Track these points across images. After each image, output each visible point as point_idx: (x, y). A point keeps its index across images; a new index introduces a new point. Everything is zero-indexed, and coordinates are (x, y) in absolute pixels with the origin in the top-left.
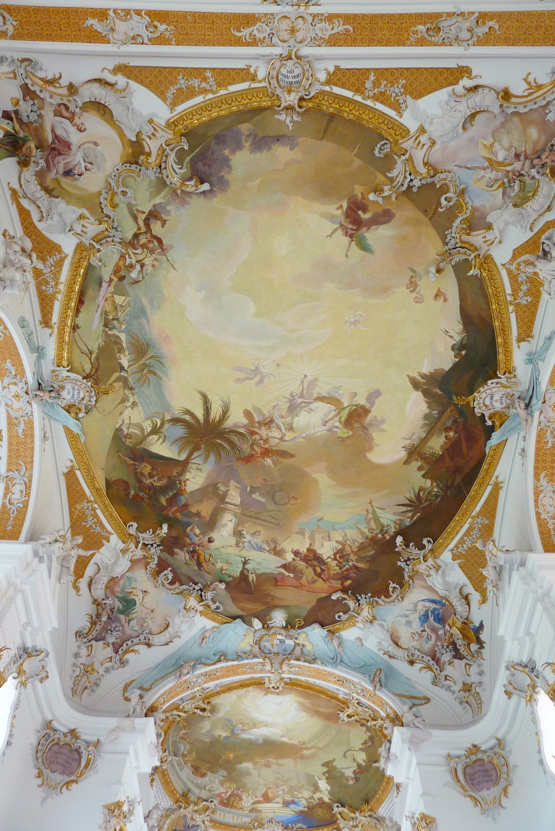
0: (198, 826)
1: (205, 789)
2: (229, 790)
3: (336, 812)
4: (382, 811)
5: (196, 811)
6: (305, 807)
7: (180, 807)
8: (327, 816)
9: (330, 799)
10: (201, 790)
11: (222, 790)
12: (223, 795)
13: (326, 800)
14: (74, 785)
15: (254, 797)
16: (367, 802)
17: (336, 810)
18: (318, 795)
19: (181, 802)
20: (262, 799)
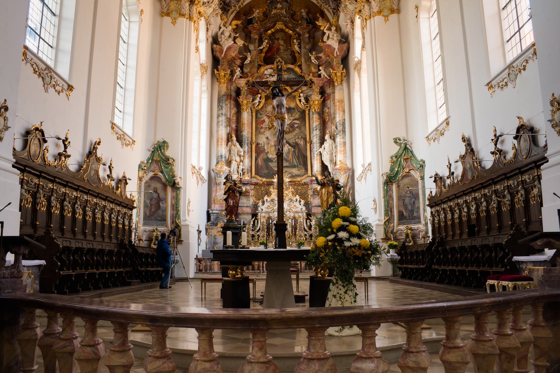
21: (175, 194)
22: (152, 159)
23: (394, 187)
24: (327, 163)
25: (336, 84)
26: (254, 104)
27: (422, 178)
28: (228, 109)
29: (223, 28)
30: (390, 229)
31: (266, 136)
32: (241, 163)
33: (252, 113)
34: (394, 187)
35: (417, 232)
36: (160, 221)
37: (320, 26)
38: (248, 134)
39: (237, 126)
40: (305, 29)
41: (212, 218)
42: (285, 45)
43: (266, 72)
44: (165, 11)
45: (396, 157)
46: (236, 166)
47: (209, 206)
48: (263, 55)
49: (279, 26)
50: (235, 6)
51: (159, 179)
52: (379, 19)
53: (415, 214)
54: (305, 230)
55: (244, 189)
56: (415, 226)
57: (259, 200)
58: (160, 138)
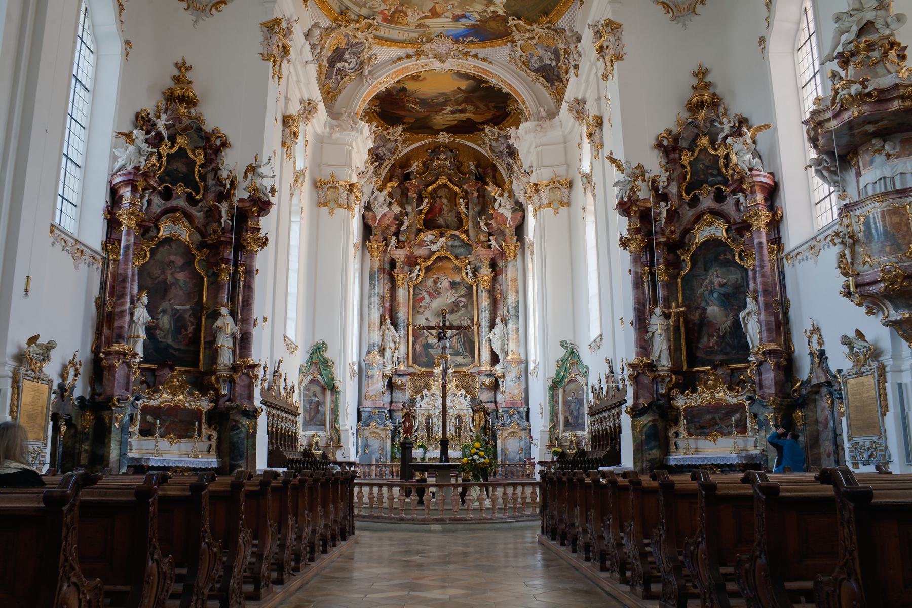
0: (362, 43)
1: (365, 7)
2: (392, 6)
3: (511, 25)
4: (562, 23)
5: (358, 29)
6: (477, 21)
7: (340, 26)
8: (501, 28)
9: (504, 12)
10: (361, 8)
11: (384, 7)
12: (386, 12)
13: (501, 13)
14: (223, 6)
15: (420, 13)
16: (546, 14)
17: (511, 22)
18: (492, 8)
19: (340, 21)
20: (429, 14)
21: (334, 397)
22: (310, 362)
23: (560, 392)
24: (497, 351)
25: (508, 259)
26: (411, 278)
27: (587, 384)
28: (382, 287)
29: (377, 193)
30: (556, 436)
31: (426, 316)
32: (397, 351)
33: (409, 288)
34: (560, 392)
35: (581, 439)
36: (320, 425)
37: (491, 191)
38: (404, 315)
39: (391, 305)
40: (474, 186)
41: (363, 416)
42: (449, 205)
43: (426, 239)
44: (322, 201)
45: (562, 361)
46: (390, 354)
47: (360, 403)
48: (423, 216)
49: (442, 181)
50: (389, 159)
51: (318, 382)
52: (548, 211)
53: (580, 421)
54: (471, 431)
55: (399, 382)
56: (579, 433)
57: (417, 393)
58: (318, 339)
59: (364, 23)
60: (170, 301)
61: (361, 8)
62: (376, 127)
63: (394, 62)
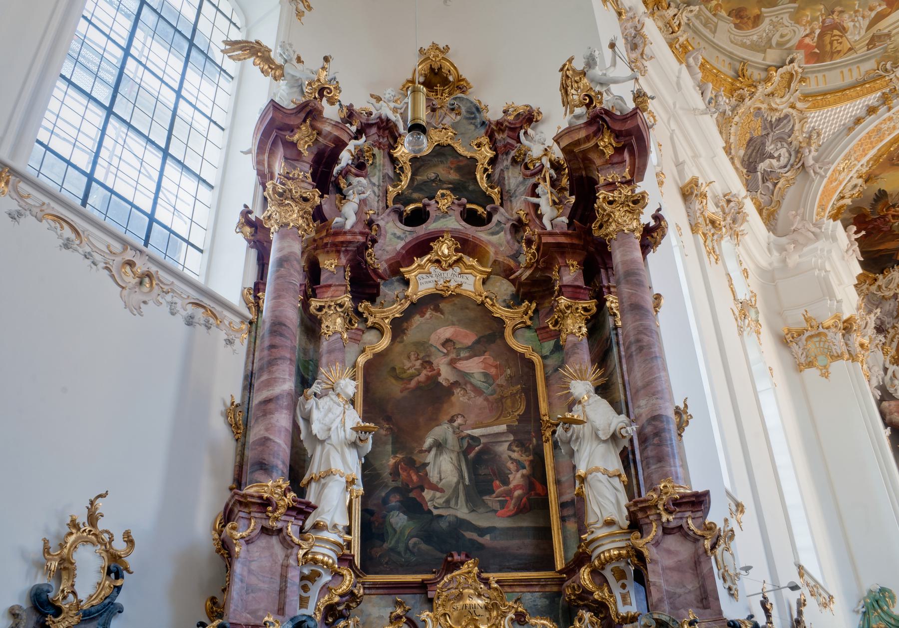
0: (786, 116)
1: (771, 47)
5: (772, 94)
10: (764, 52)
44: (803, 360)
59: (776, 76)
60: (452, 420)
61: (764, 52)
62: (856, 233)
63: (850, 129)
